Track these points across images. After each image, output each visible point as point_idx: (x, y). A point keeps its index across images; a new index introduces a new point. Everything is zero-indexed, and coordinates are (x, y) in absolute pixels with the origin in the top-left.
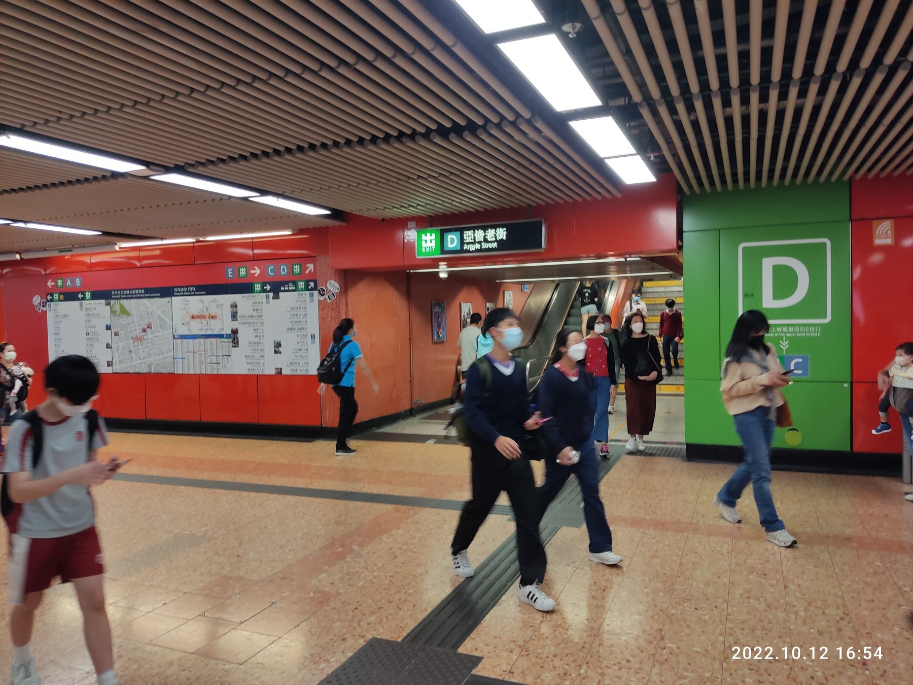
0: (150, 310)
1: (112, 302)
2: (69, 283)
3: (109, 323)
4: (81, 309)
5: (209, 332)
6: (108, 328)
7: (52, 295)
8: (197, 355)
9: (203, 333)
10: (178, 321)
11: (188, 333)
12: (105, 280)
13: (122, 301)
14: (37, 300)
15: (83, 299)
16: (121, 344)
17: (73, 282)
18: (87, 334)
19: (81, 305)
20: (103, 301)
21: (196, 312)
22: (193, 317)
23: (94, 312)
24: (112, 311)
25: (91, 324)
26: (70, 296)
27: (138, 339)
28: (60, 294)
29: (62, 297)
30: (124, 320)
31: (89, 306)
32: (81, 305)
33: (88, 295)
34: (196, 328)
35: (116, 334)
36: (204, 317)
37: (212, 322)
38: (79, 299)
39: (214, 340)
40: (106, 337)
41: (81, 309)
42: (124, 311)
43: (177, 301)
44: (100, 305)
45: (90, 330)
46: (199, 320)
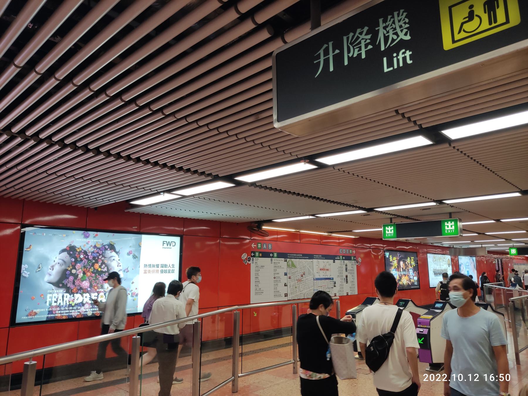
1: (288, 260)
2: (265, 247)
4: (272, 263)
5: (326, 277)
6: (286, 274)
7: (254, 253)
10: (315, 271)
12: (284, 247)
14: (244, 256)
15: (273, 257)
16: (292, 283)
17: (267, 247)
18: (275, 278)
19: (272, 260)
21: (321, 267)
23: (279, 265)
24: (288, 265)
25: (277, 272)
26: (265, 255)
27: (299, 280)
28: (260, 253)
29: (261, 255)
30: (293, 270)
31: (276, 261)
32: (272, 260)
33: (275, 255)
34: (322, 275)
35: (290, 278)
37: (327, 272)
38: (270, 257)
40: (284, 279)
41: (272, 263)
42: (293, 266)
43: (315, 261)
45: (276, 276)
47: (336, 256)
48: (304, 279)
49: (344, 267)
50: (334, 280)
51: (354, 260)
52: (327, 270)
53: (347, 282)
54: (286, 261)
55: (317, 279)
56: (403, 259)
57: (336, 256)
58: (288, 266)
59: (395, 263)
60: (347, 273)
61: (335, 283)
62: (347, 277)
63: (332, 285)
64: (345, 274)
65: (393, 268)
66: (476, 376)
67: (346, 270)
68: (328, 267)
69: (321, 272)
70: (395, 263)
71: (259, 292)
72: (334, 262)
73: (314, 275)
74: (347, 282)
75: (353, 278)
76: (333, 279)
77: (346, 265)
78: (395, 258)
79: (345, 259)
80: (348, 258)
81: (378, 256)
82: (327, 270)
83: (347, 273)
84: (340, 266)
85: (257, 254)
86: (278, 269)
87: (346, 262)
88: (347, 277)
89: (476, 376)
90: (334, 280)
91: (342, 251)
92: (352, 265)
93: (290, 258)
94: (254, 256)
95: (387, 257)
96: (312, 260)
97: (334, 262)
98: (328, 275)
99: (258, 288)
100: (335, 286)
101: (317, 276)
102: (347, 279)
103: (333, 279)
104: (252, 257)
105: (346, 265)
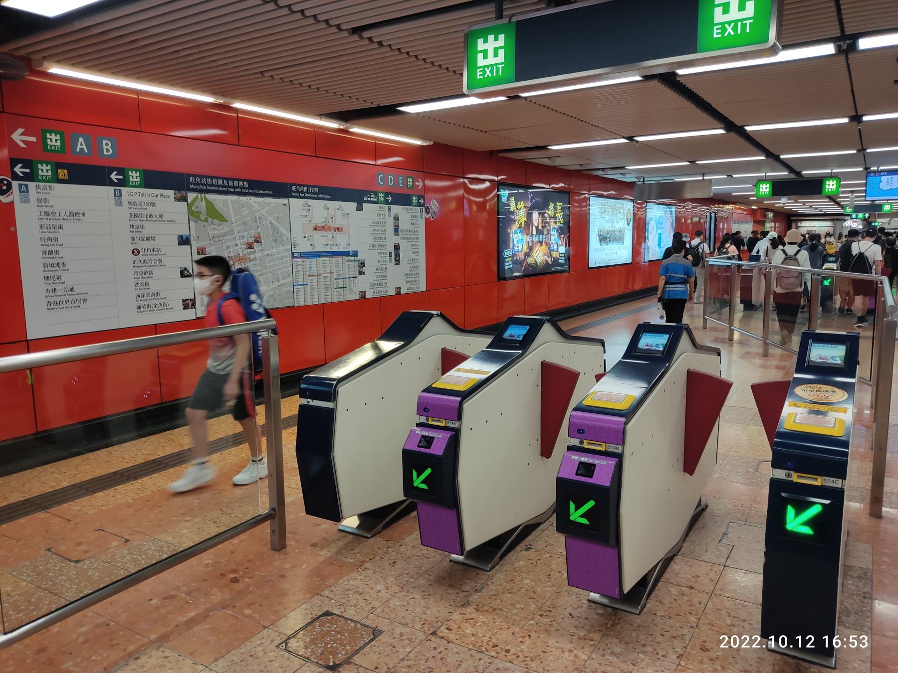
0: (258, 215)
1: (191, 196)
2: (81, 145)
3: (185, 233)
4: (119, 203)
5: (335, 249)
8: (322, 279)
9: (328, 249)
10: (297, 232)
11: (310, 249)
13: (210, 197)
15: (123, 183)
17: (95, 147)
19: (118, 195)
20: (171, 193)
21: (319, 221)
22: (316, 229)
24: (190, 212)
28: (58, 166)
32: (118, 195)
33: (134, 176)
34: (320, 242)
36: (329, 229)
37: (338, 235)
38: (111, 183)
39: (340, 259)
42: (214, 214)
43: (296, 204)
44: (164, 200)
46: (323, 233)
47: (367, 193)
48: (258, 255)
49: (390, 223)
50: (360, 257)
51: (419, 205)
52: (339, 229)
53: (398, 261)
54: (184, 199)
55: (305, 255)
56: (541, 205)
57: (367, 193)
58: (193, 214)
59: (521, 216)
60: (397, 240)
61: (362, 265)
62: (397, 248)
63: (354, 269)
64: (392, 240)
65: (515, 227)
66: (810, 639)
67: (396, 230)
68: (339, 221)
69: (318, 235)
70: (521, 216)
71: (63, 299)
72: (360, 208)
73: (293, 245)
74: (398, 261)
75: (416, 252)
76: (355, 254)
77: (396, 219)
78: (521, 205)
79: (394, 203)
80: (402, 199)
81: (485, 202)
82: (339, 229)
83: (397, 240)
84: (377, 219)
85: (45, 170)
86: (146, 224)
87: (397, 209)
88: (397, 248)
89: (810, 639)
90: (360, 257)
91: (385, 180)
92: (413, 220)
93: (201, 191)
94: (31, 177)
95: (504, 199)
96: (285, 201)
97: (360, 208)
98: (341, 243)
99: (60, 288)
100: (361, 273)
101: (304, 247)
102: (397, 255)
103: (355, 254)
104: (15, 177)
105: (396, 219)
